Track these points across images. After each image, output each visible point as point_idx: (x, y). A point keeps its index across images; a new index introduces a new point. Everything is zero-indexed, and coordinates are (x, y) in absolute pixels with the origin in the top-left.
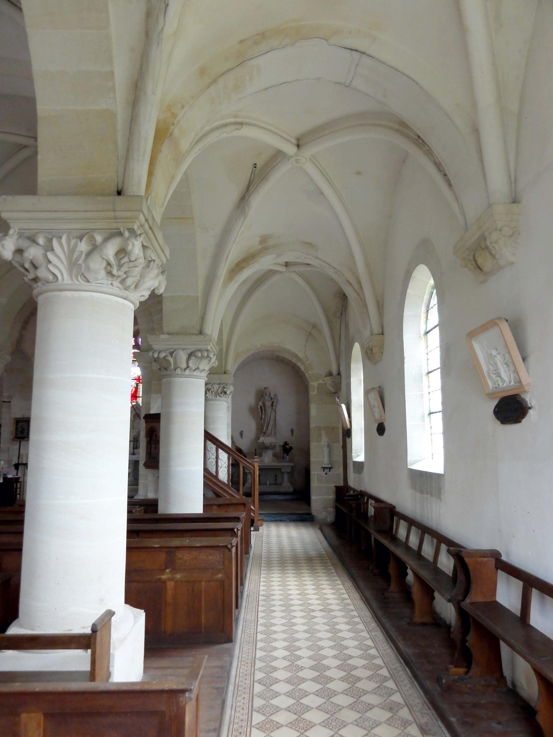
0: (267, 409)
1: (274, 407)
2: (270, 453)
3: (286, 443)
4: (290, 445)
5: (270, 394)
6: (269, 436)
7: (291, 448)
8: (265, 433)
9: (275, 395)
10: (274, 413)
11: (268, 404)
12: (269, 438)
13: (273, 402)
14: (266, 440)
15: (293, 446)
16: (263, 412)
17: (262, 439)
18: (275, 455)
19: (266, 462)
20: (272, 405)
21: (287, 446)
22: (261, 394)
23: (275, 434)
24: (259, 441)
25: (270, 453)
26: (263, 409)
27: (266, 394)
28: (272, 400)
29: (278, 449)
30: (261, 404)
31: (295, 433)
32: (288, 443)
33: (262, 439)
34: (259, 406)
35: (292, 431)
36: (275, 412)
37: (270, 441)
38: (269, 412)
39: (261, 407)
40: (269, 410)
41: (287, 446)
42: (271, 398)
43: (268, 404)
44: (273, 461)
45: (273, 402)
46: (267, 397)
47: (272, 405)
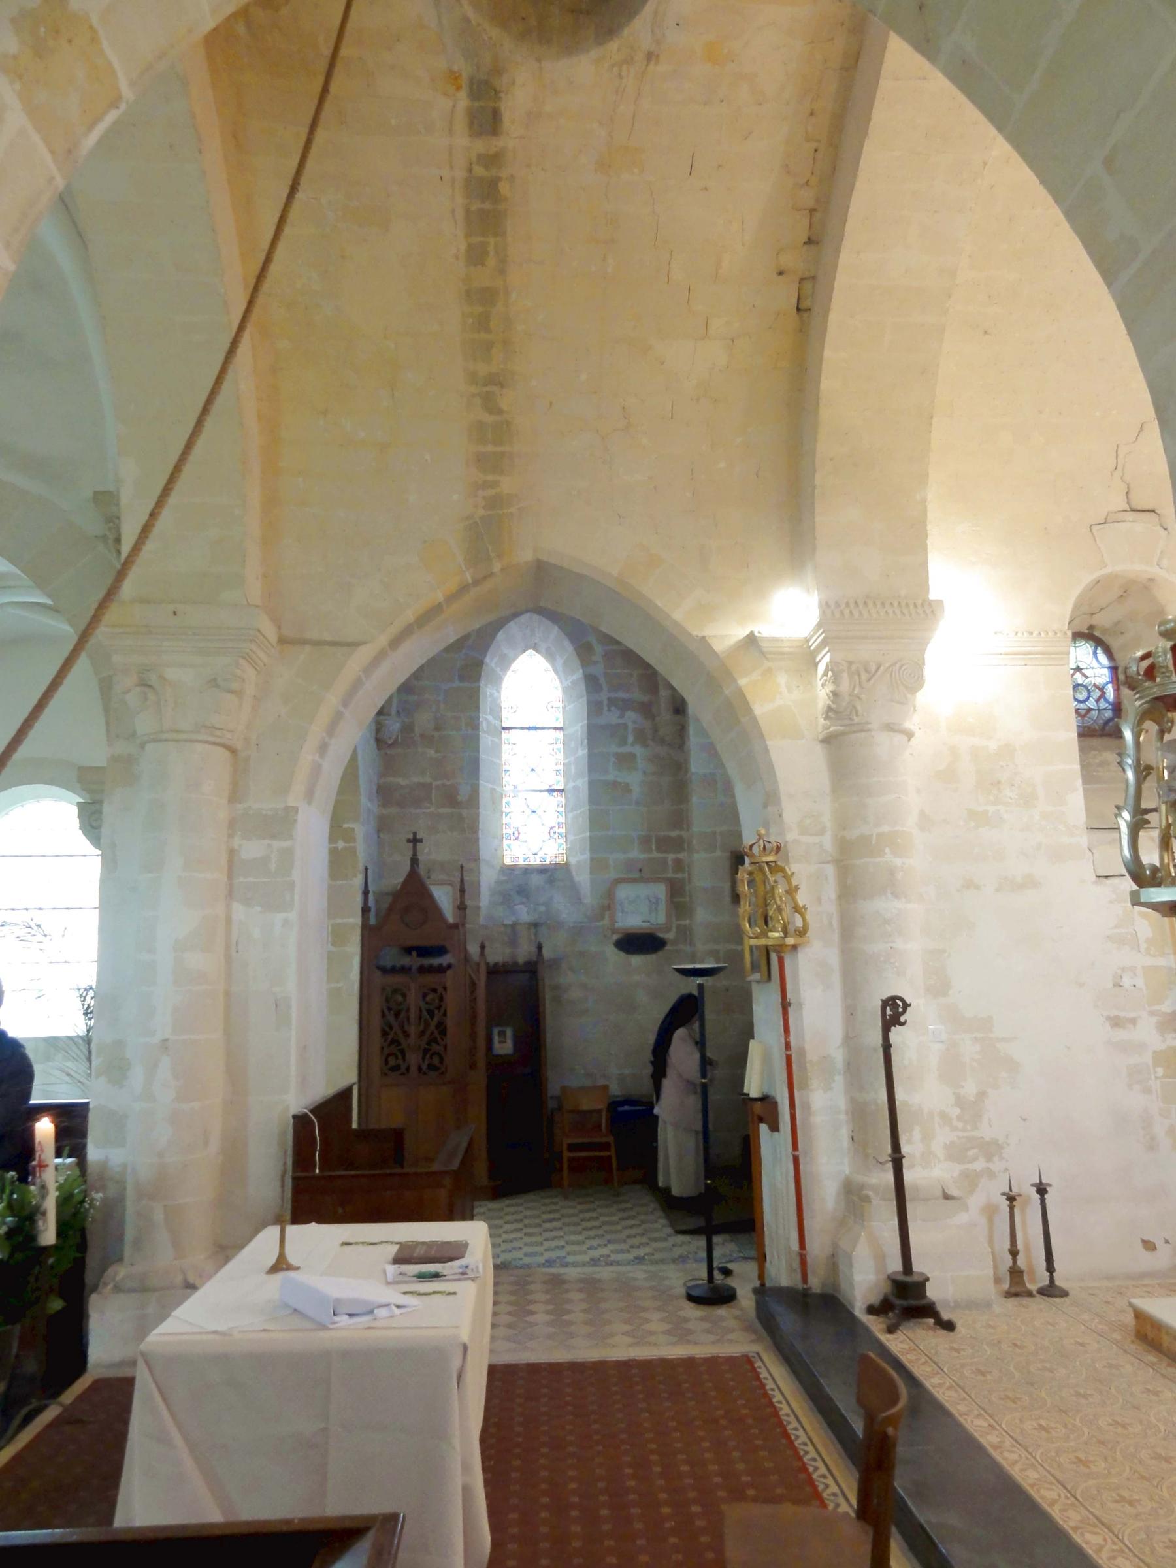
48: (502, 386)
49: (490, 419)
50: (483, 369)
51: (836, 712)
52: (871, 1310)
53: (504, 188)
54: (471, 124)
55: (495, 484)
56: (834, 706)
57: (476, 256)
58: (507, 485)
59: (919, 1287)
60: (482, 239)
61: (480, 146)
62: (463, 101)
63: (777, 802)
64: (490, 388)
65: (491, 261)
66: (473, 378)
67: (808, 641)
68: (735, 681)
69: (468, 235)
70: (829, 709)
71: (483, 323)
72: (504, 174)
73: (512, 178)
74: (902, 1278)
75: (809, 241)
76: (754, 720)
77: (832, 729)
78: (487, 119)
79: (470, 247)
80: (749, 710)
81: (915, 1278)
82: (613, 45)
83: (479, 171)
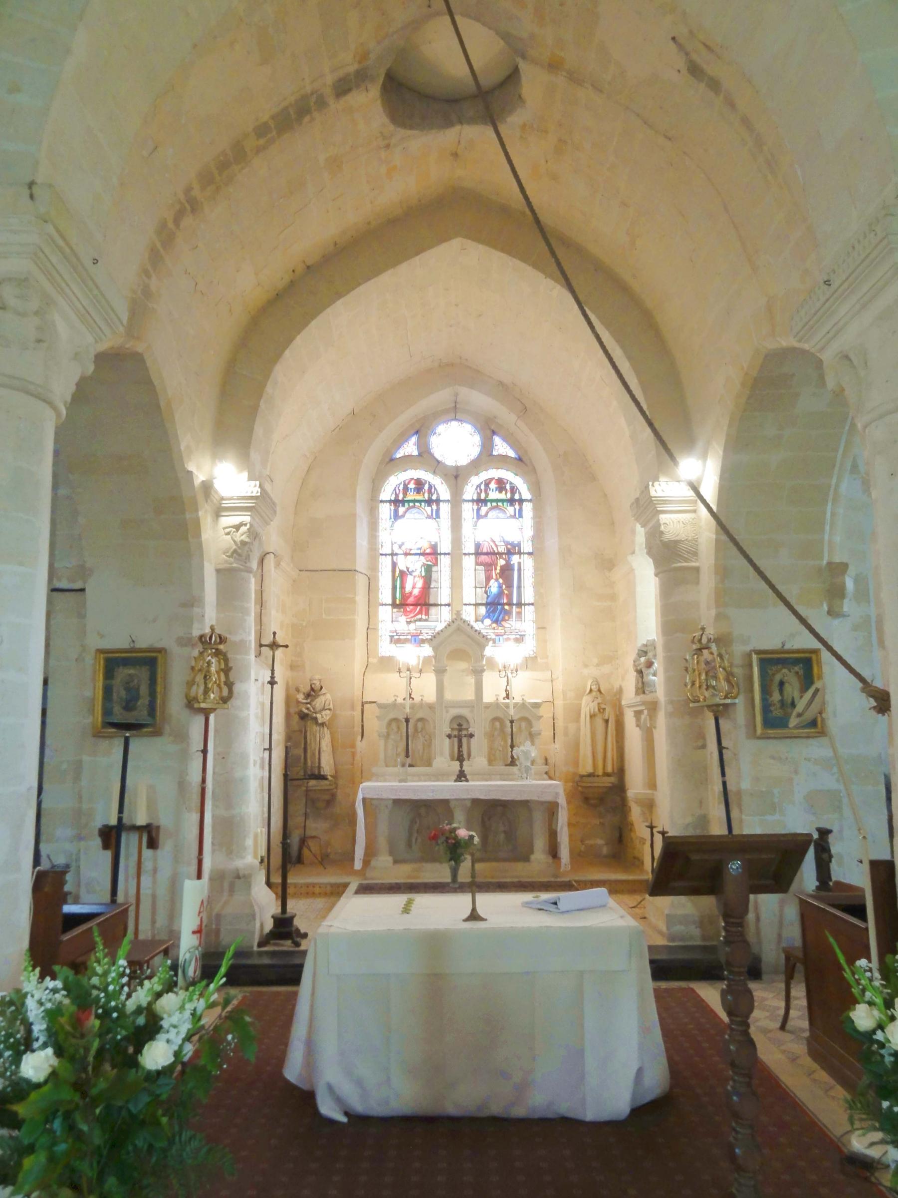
48: (193, 211)
49: (171, 225)
50: (196, 192)
51: (240, 555)
52: (260, 945)
53: (307, 119)
54: (340, 80)
55: (149, 277)
56: (239, 551)
57: (262, 130)
58: (154, 283)
59: (291, 919)
60: (273, 126)
61: (328, 91)
62: (352, 68)
63: (203, 607)
64: (190, 205)
65: (262, 141)
66: (188, 190)
67: (222, 499)
68: (197, 510)
69: (273, 117)
70: (235, 551)
71: (223, 165)
72: (316, 114)
73: (312, 120)
74: (280, 916)
75: (308, 267)
76: (200, 546)
77: (235, 565)
78: (343, 88)
79: (265, 124)
80: (198, 535)
81: (288, 915)
82: (392, 127)
83: (313, 99)
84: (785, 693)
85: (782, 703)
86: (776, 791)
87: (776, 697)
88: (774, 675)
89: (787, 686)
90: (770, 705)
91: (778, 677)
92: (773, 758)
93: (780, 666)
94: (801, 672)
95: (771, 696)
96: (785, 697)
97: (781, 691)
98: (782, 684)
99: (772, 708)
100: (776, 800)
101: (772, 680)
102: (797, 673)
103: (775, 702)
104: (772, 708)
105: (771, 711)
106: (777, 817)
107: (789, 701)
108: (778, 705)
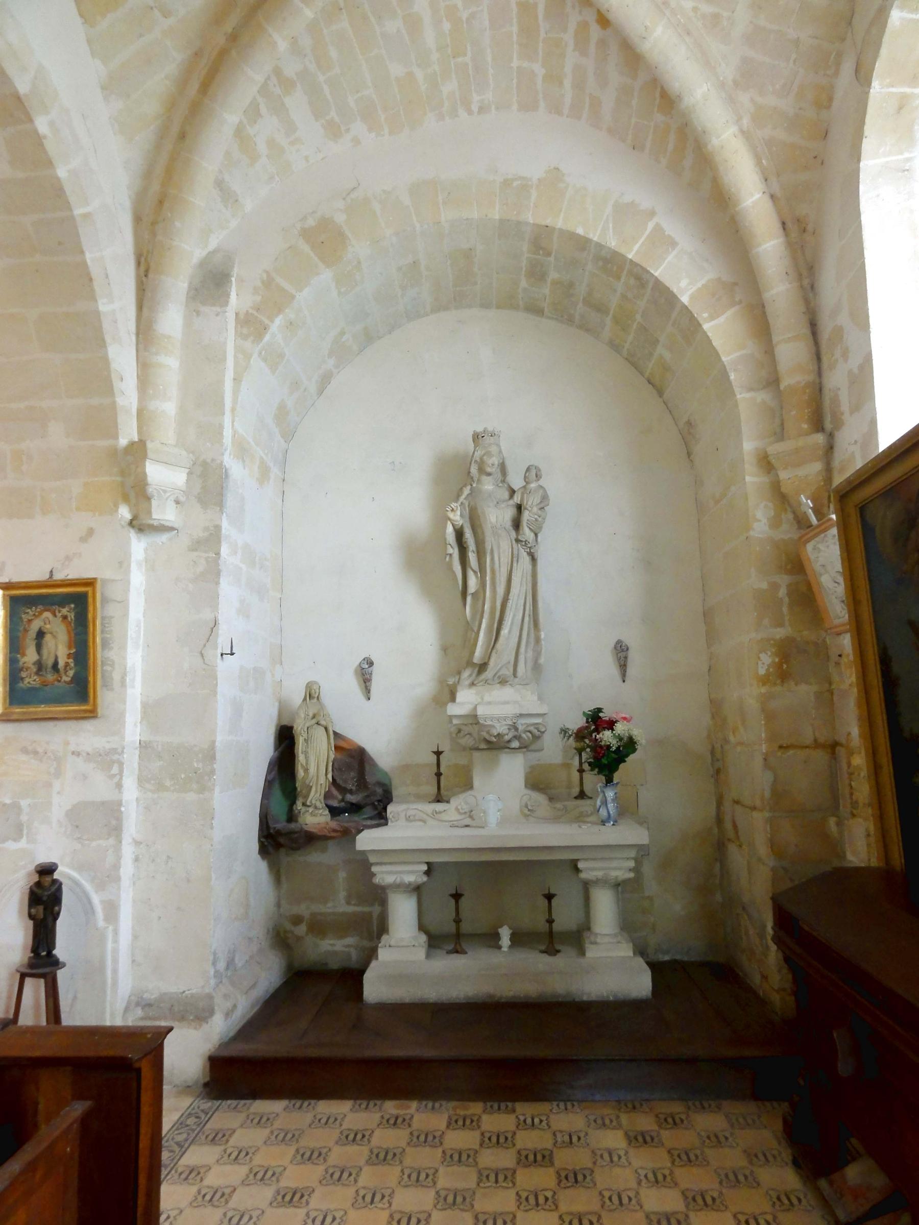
0: (489, 541)
1: (527, 534)
2: (512, 769)
3: (597, 721)
4: (620, 728)
5: (503, 468)
6: (503, 682)
7: (629, 745)
8: (482, 667)
9: (533, 473)
10: (525, 559)
11: (497, 516)
12: (507, 693)
13: (519, 508)
14: (493, 703)
15: (638, 734)
16: (472, 557)
17: (467, 700)
18: (537, 782)
19: (493, 818)
20: (517, 524)
21: (606, 736)
22: (461, 473)
23: (537, 667)
24: (453, 710)
25: (512, 769)
26: (467, 543)
27: (481, 471)
28: (517, 499)
29: (554, 750)
30: (457, 517)
31: (631, 671)
32: (605, 716)
33: (467, 700)
34: (450, 529)
35: (621, 652)
36: (533, 559)
37: (510, 710)
38: (505, 559)
39: (459, 534)
40: (501, 547)
41: (606, 736)
42: (512, 492)
43: (497, 516)
44: (528, 812)
45: (519, 508)
46: (488, 485)
47: (517, 524)
84: (45, 652)
85: (40, 666)
86: (24, 803)
87: (30, 656)
88: (30, 621)
89: (48, 637)
90: (21, 670)
91: (36, 625)
92: (25, 751)
93: (40, 607)
94: (71, 616)
95: (24, 655)
96: (45, 657)
97: (39, 648)
98: (41, 634)
99: (23, 674)
100: (24, 818)
101: (26, 631)
102: (65, 618)
103: (30, 665)
104: (23, 674)
105: (22, 679)
106: (23, 844)
107: (50, 662)
108: (34, 669)
